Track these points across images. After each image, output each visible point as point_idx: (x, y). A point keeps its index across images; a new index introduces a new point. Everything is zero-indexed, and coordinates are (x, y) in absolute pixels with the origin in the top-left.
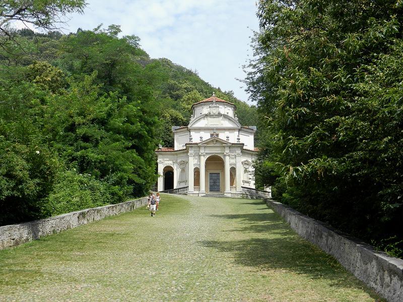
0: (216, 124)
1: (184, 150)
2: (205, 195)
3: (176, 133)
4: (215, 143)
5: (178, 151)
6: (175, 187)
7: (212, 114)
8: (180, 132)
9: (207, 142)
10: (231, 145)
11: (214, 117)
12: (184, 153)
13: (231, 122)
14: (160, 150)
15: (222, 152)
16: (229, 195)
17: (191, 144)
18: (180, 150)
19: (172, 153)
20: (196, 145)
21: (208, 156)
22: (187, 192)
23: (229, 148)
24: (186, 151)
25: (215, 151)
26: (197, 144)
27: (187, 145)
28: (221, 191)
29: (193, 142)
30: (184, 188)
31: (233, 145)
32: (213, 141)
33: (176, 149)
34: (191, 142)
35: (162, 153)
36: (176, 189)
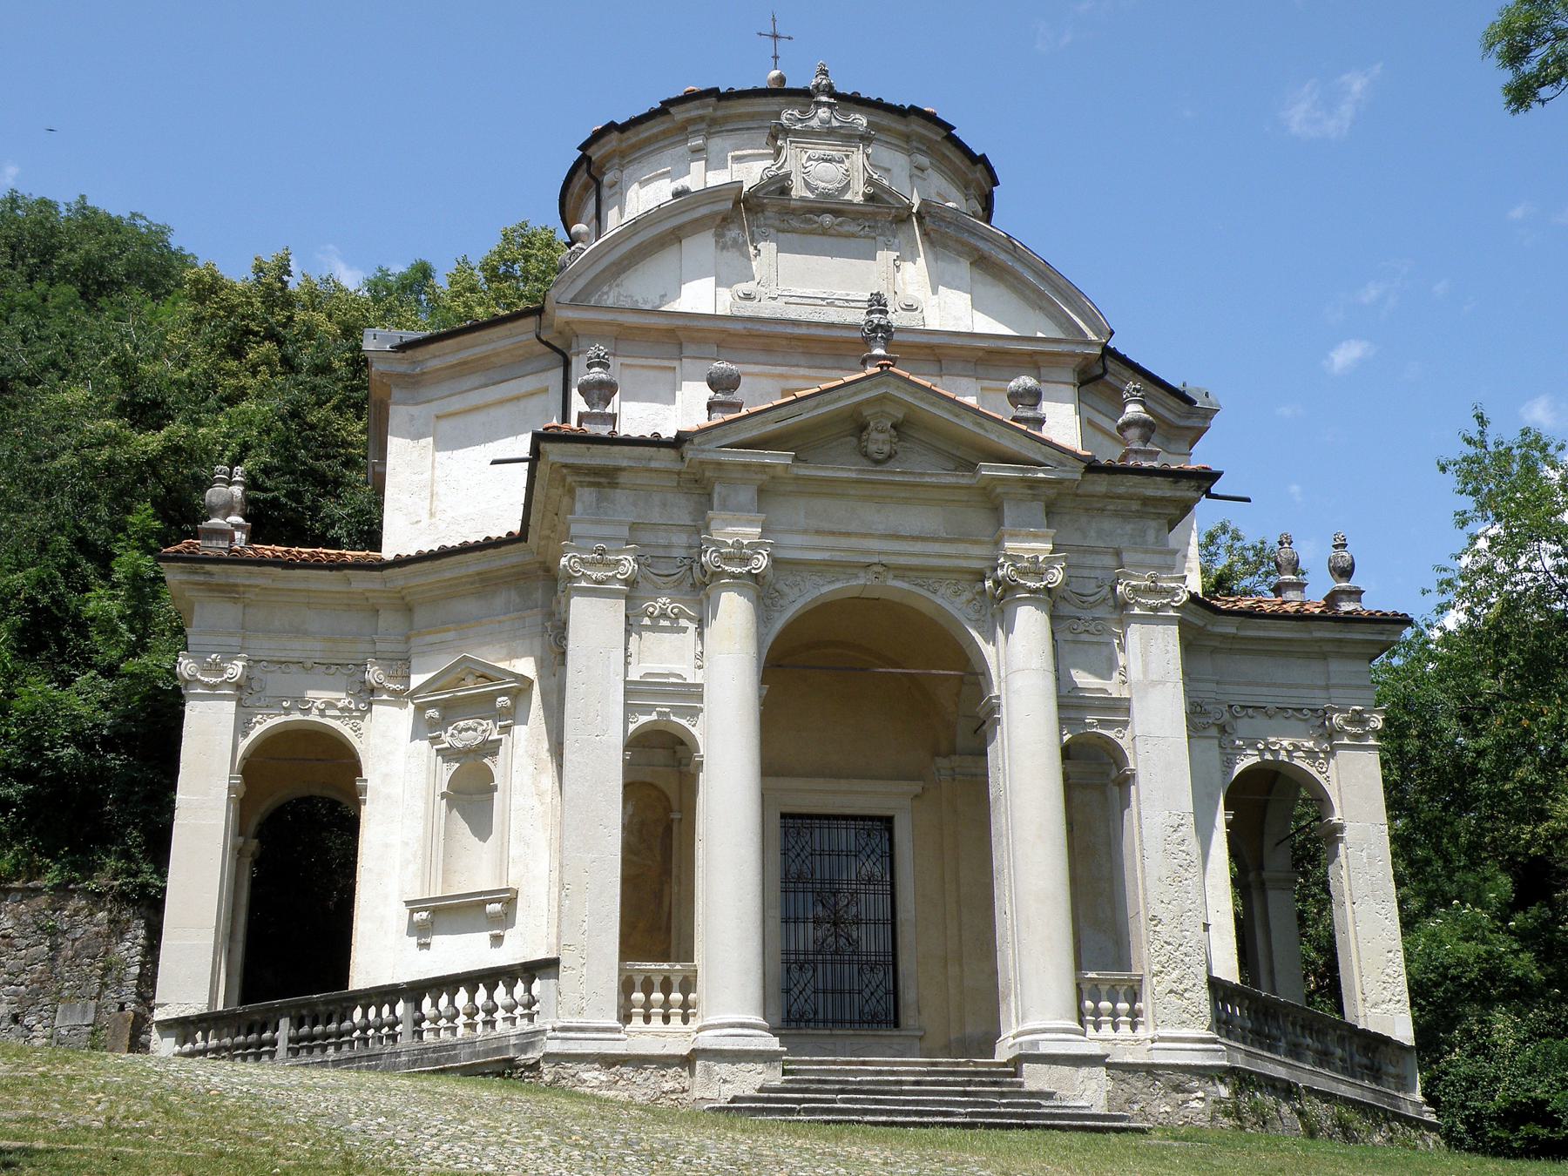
0: (840, 293)
1: (489, 544)
2: (775, 1077)
3: (413, 382)
4: (878, 442)
5: (421, 558)
6: (381, 951)
7: (798, 191)
8: (462, 370)
9: (800, 437)
10: (1075, 473)
11: (824, 232)
12: (487, 584)
13: (997, 292)
14: (217, 547)
15: (972, 555)
16: (1089, 1093)
17: (613, 441)
18: (465, 549)
19: (361, 582)
20: (665, 458)
21: (798, 599)
22: (529, 1040)
23: (1051, 511)
24: (512, 556)
25: (881, 538)
26: (681, 440)
27: (553, 452)
28: (908, 1017)
29: (625, 429)
30: (491, 977)
31: (1101, 484)
32: (856, 425)
33: (399, 539)
34: (604, 431)
35: (239, 575)
36: (388, 994)
